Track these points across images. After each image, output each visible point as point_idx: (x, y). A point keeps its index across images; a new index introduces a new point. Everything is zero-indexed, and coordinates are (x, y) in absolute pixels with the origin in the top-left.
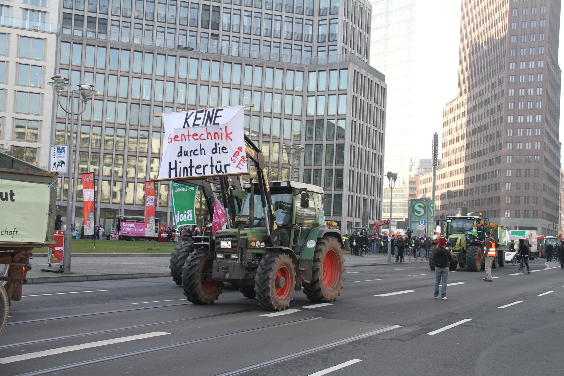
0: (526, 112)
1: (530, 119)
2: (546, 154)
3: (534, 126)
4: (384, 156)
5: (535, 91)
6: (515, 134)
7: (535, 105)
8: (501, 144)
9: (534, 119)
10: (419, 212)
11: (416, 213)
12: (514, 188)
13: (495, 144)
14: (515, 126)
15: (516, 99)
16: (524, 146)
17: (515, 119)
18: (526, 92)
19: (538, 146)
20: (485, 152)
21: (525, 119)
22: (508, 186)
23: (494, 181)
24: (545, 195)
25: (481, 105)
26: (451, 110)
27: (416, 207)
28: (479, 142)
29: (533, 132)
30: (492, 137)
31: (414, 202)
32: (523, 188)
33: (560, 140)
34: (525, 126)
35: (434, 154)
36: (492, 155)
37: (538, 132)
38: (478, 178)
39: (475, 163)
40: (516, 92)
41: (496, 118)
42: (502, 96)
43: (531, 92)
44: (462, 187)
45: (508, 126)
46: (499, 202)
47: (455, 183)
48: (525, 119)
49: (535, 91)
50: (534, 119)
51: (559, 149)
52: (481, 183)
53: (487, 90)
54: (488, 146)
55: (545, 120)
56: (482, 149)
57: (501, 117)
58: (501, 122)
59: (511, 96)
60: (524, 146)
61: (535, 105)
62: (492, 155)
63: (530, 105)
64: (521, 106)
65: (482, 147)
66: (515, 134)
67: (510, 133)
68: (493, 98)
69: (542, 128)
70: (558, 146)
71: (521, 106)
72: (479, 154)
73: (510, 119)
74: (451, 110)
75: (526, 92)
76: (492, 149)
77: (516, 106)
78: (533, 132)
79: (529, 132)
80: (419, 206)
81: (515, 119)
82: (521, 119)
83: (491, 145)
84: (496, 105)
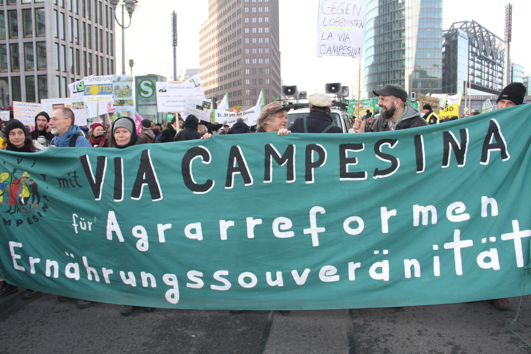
0: (258, 25)
1: (261, 30)
2: (273, 58)
3: (264, 35)
4: (115, 34)
5: (264, 9)
6: (251, 41)
7: (264, 20)
8: (241, 50)
9: (264, 30)
10: (146, 93)
11: (142, 94)
12: (252, 83)
13: (236, 50)
14: (250, 36)
15: (251, 15)
16: (258, 51)
17: (251, 30)
18: (257, 10)
19: (267, 51)
20: (230, 57)
21: (257, 30)
22: (248, 82)
23: (237, 78)
24: (273, 88)
25: (225, 22)
26: (205, 28)
27: (143, 87)
28: (225, 50)
29: (264, 40)
30: (234, 45)
31: (139, 81)
32: (258, 83)
33: (280, 50)
34: (258, 36)
35: (174, 34)
36: (235, 59)
37: (267, 40)
38: (226, 77)
39: (223, 66)
40: (250, 10)
41: (236, 30)
42: (240, 12)
43: (261, 9)
44: (216, 85)
45: (246, 36)
46: (241, 94)
47: (210, 83)
48: (257, 30)
49: (264, 9)
50: (264, 30)
51: (279, 56)
52: (228, 81)
53: (229, 9)
54: (232, 53)
55: (271, 31)
56: (227, 55)
57: (240, 29)
58: (240, 33)
59: (247, 13)
60: (258, 51)
61: (264, 20)
62: (235, 59)
63: (260, 20)
64: (254, 20)
65: (227, 54)
66: (251, 41)
67: (247, 41)
68: (234, 15)
69: (270, 37)
70: (279, 53)
71: (254, 20)
72: (226, 59)
73: (247, 30)
74: (205, 28)
75: (257, 10)
76: (234, 54)
77: (250, 20)
78: (264, 40)
79: (261, 40)
80: (146, 85)
81: (251, 30)
82: (254, 30)
83: (234, 51)
84: (236, 20)
